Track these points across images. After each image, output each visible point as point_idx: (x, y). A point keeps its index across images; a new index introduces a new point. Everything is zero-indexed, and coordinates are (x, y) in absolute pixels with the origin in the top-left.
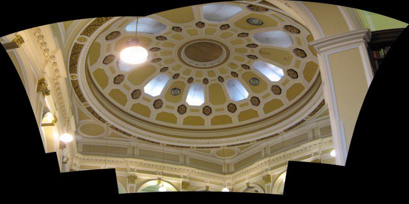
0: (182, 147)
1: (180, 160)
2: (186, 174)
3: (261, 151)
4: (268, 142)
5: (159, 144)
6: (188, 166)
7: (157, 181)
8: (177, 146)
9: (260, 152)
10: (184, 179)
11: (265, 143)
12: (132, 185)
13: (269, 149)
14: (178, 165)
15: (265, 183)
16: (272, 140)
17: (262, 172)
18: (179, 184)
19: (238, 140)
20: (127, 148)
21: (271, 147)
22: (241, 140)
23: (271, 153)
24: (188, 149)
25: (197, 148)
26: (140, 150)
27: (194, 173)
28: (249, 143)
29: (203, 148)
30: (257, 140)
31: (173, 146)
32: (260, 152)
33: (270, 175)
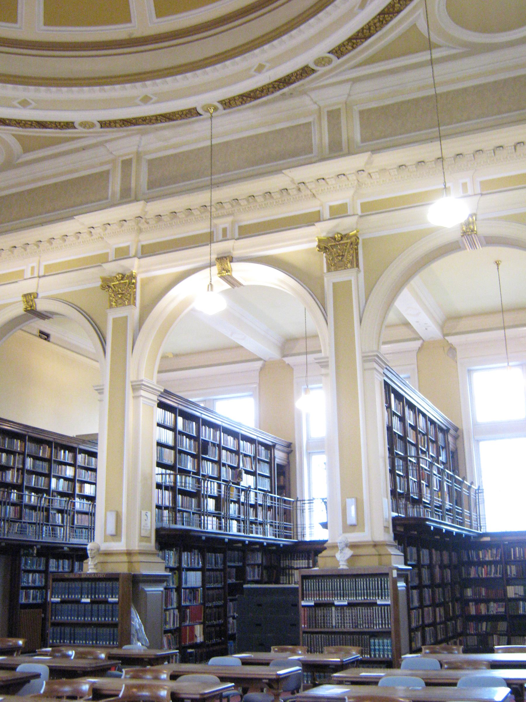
3: (107, 172)
4: (145, 139)
9: (104, 176)
11: (135, 139)
13: (144, 169)
15: (111, 306)
16: (167, 133)
17: (103, 259)
19: (24, 104)
21: (151, 163)
22: (41, 105)
23: (151, 185)
28: (69, 125)
30: (105, 124)
32: (104, 176)
33: (132, 277)
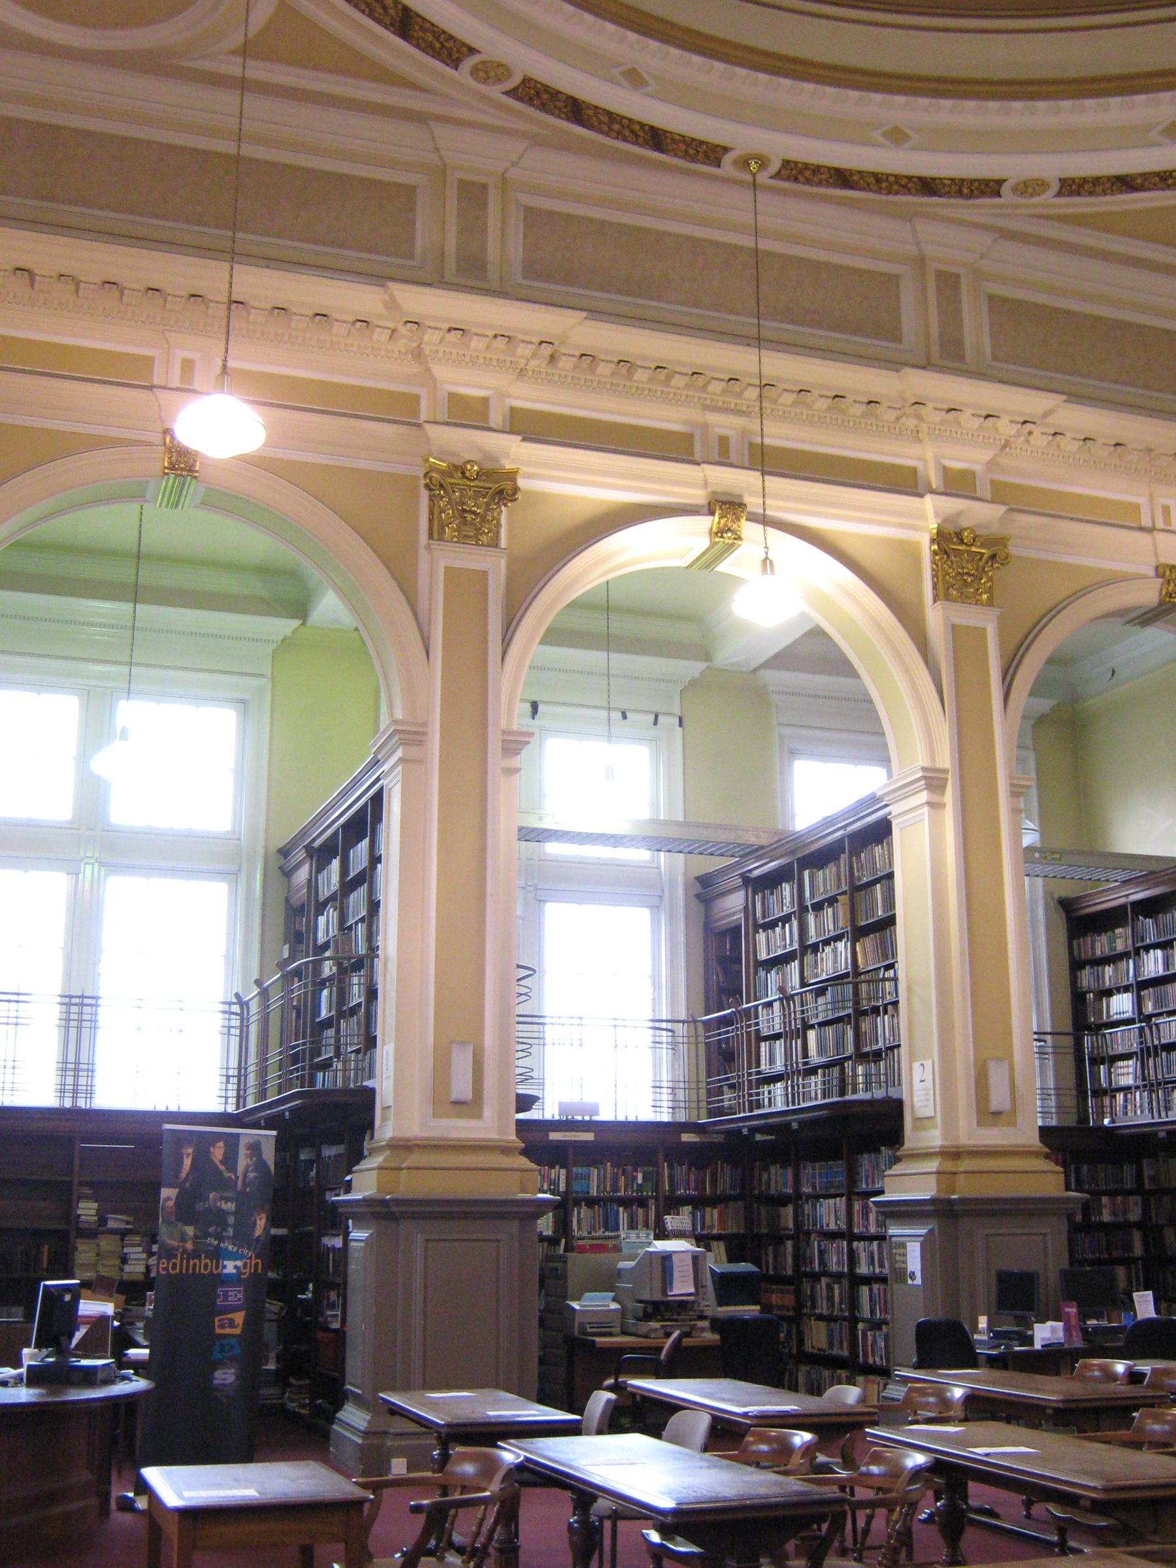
0: (928, 186)
1: (909, 320)
2: (963, 458)
5: (711, 153)
6: (980, 374)
7: (705, 523)
8: (882, 182)
10: (952, 505)
12: (471, 558)
14: (895, 364)
18: (909, 551)
20: (410, 191)
24: (980, 209)
25: (1071, 187)
26: (532, 216)
27: (1039, 440)
29: (1126, 183)
31: (842, 178)
